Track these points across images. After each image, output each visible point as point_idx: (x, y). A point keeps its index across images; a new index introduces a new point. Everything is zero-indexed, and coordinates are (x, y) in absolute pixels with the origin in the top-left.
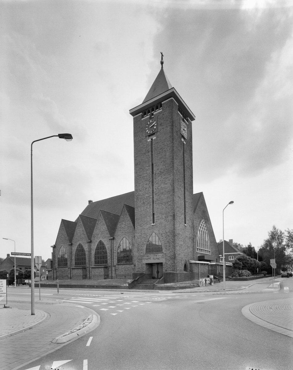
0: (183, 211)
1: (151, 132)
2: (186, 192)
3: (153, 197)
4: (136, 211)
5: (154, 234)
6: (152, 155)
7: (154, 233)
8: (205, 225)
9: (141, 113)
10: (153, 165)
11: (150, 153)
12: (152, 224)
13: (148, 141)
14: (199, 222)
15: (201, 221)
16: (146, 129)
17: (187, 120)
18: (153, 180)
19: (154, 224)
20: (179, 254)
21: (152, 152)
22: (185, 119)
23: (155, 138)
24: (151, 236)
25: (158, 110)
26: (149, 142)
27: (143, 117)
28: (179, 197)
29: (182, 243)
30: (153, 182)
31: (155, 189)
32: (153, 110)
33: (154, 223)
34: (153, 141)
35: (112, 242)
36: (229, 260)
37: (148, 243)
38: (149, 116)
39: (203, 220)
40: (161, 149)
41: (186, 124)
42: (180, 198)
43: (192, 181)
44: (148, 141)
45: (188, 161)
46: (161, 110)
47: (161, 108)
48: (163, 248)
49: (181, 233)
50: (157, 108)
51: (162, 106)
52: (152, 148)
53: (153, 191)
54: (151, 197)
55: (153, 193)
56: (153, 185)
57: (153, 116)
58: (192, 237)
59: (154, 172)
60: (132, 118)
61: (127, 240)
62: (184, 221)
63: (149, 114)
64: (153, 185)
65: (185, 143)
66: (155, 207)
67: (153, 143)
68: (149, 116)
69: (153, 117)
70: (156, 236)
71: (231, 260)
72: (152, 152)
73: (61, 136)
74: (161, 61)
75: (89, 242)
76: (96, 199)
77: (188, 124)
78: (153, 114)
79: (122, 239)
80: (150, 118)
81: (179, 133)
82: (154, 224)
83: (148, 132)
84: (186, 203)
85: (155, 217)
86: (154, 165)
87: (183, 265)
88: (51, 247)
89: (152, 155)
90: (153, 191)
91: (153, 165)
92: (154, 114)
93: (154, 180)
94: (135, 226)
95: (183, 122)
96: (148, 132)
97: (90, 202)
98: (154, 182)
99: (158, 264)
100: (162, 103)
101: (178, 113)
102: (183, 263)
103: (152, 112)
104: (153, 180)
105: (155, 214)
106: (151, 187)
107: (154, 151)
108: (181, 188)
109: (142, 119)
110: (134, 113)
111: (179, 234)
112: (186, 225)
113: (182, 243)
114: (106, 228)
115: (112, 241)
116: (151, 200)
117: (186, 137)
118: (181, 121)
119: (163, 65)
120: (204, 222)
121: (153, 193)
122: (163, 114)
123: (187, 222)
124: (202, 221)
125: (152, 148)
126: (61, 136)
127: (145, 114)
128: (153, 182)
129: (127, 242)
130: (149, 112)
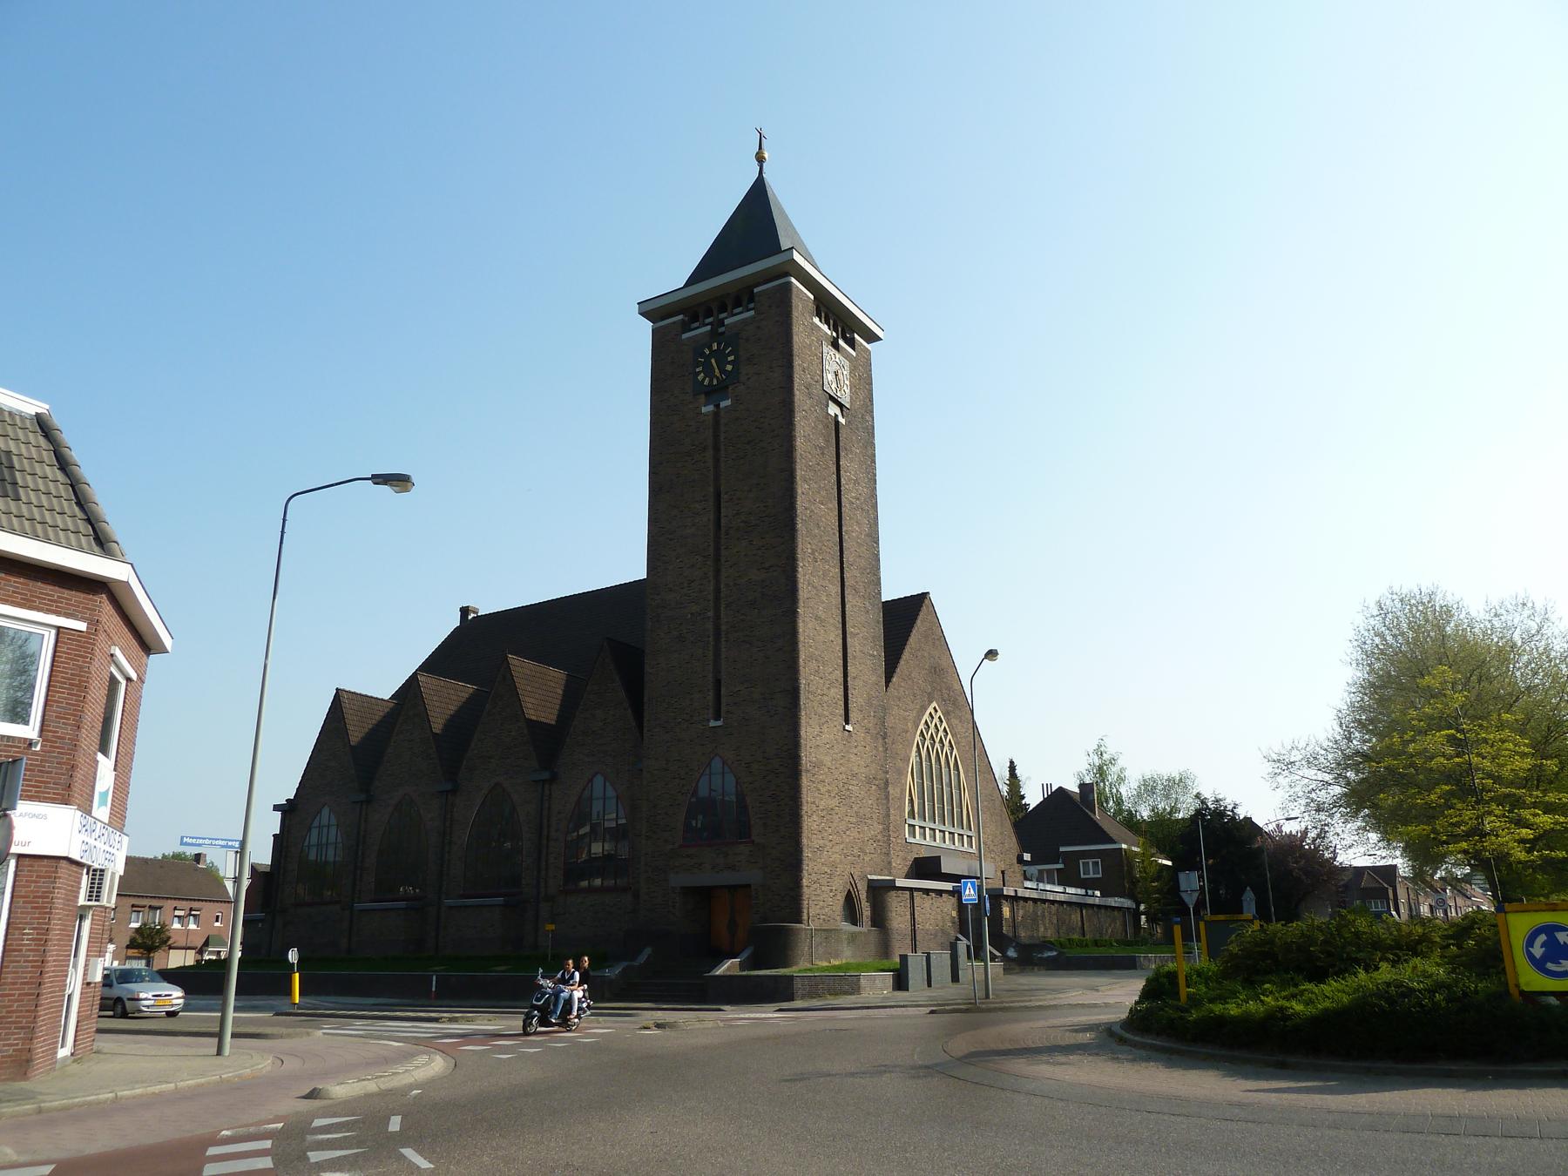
0: (839, 674)
1: (715, 382)
2: (848, 598)
3: (717, 617)
4: (647, 668)
5: (717, 764)
6: (717, 461)
7: (717, 758)
8: (944, 724)
9: (681, 317)
10: (718, 496)
11: (710, 453)
12: (713, 723)
13: (704, 410)
14: (915, 713)
15: (926, 709)
16: (697, 370)
17: (851, 343)
18: (717, 549)
19: (719, 723)
20: (821, 849)
21: (717, 449)
22: (841, 342)
23: (728, 402)
24: (707, 771)
25: (740, 309)
26: (705, 415)
27: (686, 327)
28: (817, 618)
29: (834, 803)
30: (717, 559)
31: (727, 585)
32: (723, 309)
33: (717, 718)
34: (722, 413)
35: (547, 792)
36: (1082, 876)
37: (693, 800)
38: (709, 328)
39: (934, 704)
40: (749, 443)
41: (847, 356)
42: (822, 621)
43: (878, 555)
44: (704, 410)
45: (856, 482)
46: (752, 313)
47: (752, 305)
48: (752, 822)
49: (827, 760)
50: (738, 303)
51: (756, 299)
52: (716, 436)
53: (717, 591)
54: (710, 614)
55: (717, 599)
56: (717, 572)
57: (722, 330)
58: (881, 775)
59: (723, 521)
60: (647, 326)
61: (607, 784)
62: (842, 712)
63: (710, 320)
64: (717, 572)
65: (842, 420)
66: (723, 656)
67: (723, 421)
68: (709, 328)
69: (724, 333)
70: (726, 768)
71: (1091, 876)
72: (717, 449)
73: (379, 479)
74: (757, 153)
75: (447, 791)
76: (488, 604)
77: (854, 354)
78: (721, 323)
79: (591, 781)
80: (714, 335)
81: (816, 391)
82: (719, 723)
83: (704, 380)
84: (849, 640)
85: (722, 692)
86: (724, 497)
87: (841, 898)
88: (276, 808)
89: (717, 461)
90: (717, 591)
91: (718, 496)
92: (726, 322)
93: (723, 552)
94: (645, 731)
95: (833, 351)
96: (704, 380)
97: (465, 611)
98: (723, 559)
99: (733, 888)
100: (756, 290)
101: (813, 323)
102: (839, 886)
103: (722, 316)
104: (717, 549)
105: (723, 682)
106: (711, 578)
107: (722, 447)
108: (826, 583)
109: (685, 336)
110: (653, 311)
111: (818, 765)
112: (848, 727)
113: (834, 803)
114: (526, 731)
115: (547, 786)
116: (710, 626)
117: (848, 399)
118: (828, 351)
119: (764, 164)
120: (939, 713)
121: (717, 599)
122: (759, 327)
123: (853, 715)
124: (930, 709)
125: (716, 436)
126: (379, 479)
127: (695, 318)
128: (717, 559)
129: (610, 792)
130: (709, 313)
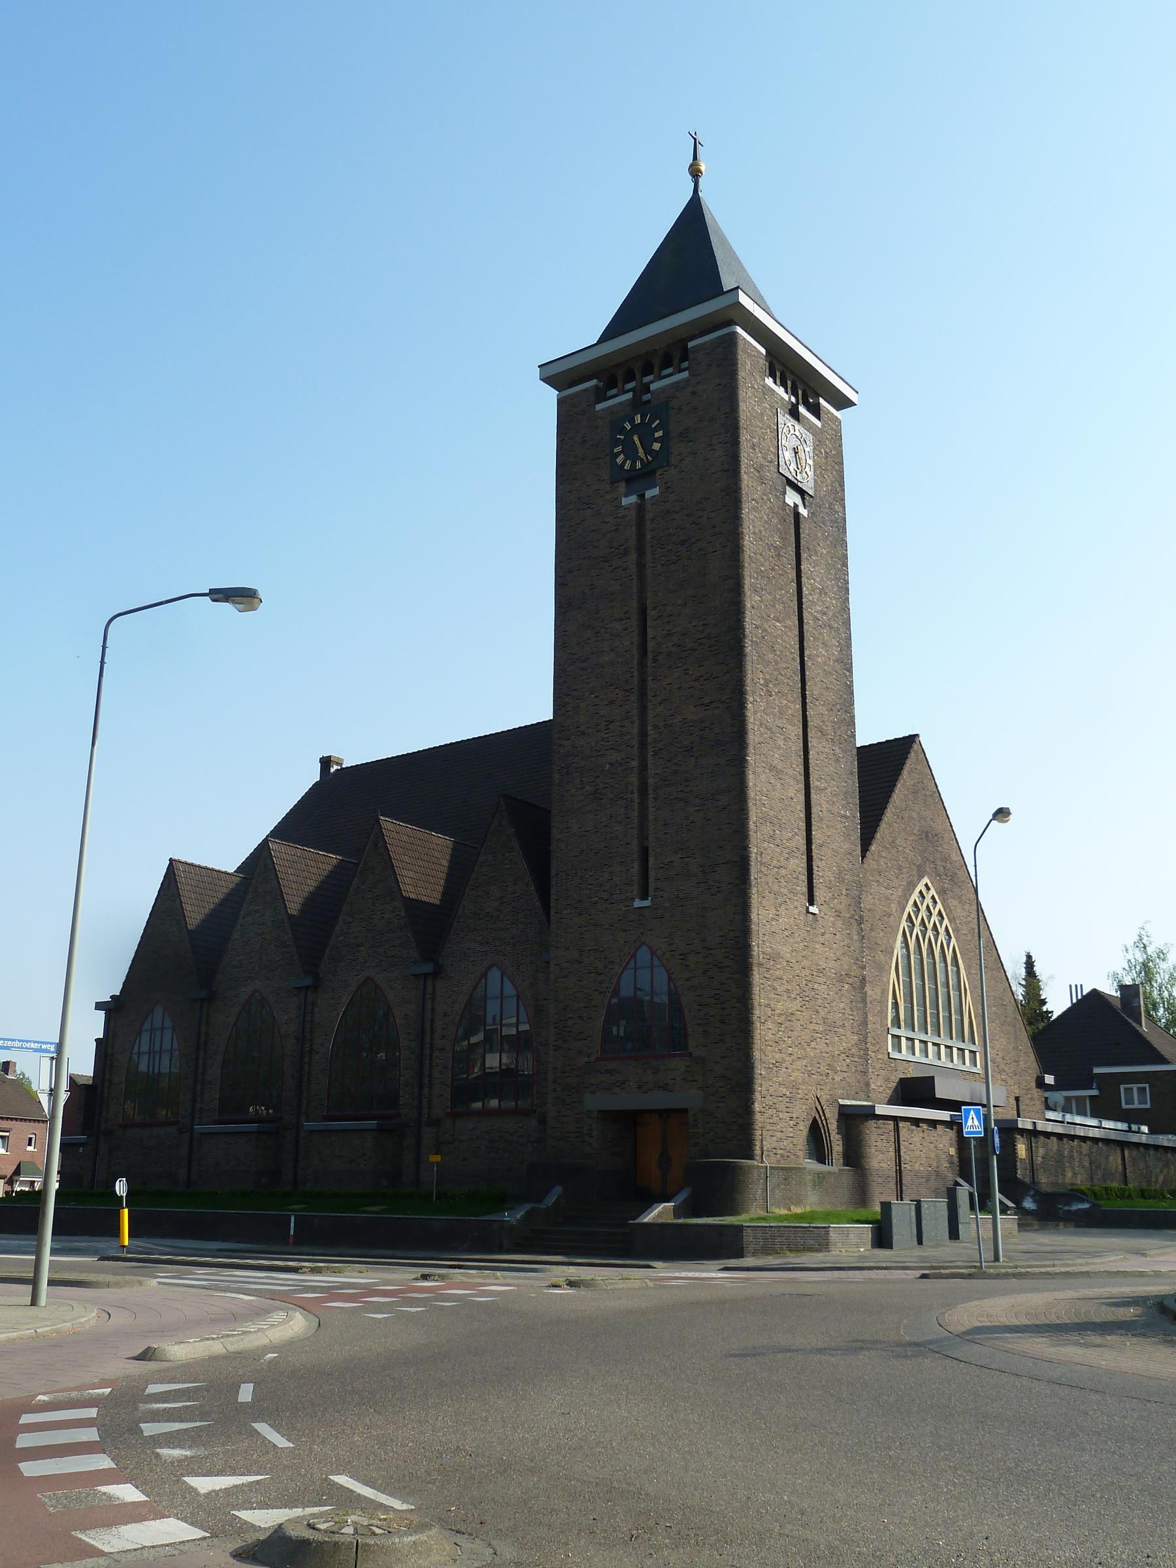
0: (801, 841)
1: (638, 465)
2: (812, 742)
3: (643, 768)
4: (555, 834)
5: (644, 955)
6: (641, 566)
7: (645, 948)
8: (939, 906)
9: (594, 382)
10: (643, 612)
11: (633, 557)
12: (638, 903)
13: (625, 501)
14: (900, 892)
15: (915, 886)
16: (616, 450)
17: (816, 410)
18: (643, 681)
19: (647, 903)
20: (777, 1064)
21: (641, 552)
24: (632, 964)
27: (600, 395)
28: (772, 768)
29: (794, 1006)
30: (643, 694)
31: (656, 727)
32: (648, 369)
33: (644, 896)
34: (648, 505)
35: (430, 989)
36: (1124, 1106)
37: (615, 1001)
38: (629, 395)
39: (926, 880)
40: (683, 543)
41: (810, 427)
42: (779, 772)
44: (625, 501)
45: (823, 592)
46: (686, 374)
47: (685, 365)
48: (690, 1029)
49: (785, 951)
50: (667, 362)
51: (691, 356)
52: (641, 536)
53: (643, 734)
54: (635, 764)
55: (643, 745)
56: (643, 709)
58: (855, 971)
60: (551, 395)
61: (505, 979)
62: (805, 890)
64: (643, 709)
65: (803, 511)
66: (651, 818)
67: (649, 516)
68: (629, 395)
70: (656, 962)
71: (1136, 1105)
72: (641, 552)
73: (220, 595)
74: (691, 166)
75: (307, 988)
78: (646, 388)
79: (484, 975)
80: (637, 404)
81: (770, 474)
82: (647, 903)
83: (624, 463)
84: (813, 796)
86: (651, 614)
87: (804, 1129)
88: (99, 1006)
89: (641, 566)
90: (643, 734)
91: (643, 612)
92: (653, 387)
93: (650, 684)
94: (552, 913)
95: (791, 422)
96: (624, 463)
97: (326, 762)
99: (665, 1114)
100: (691, 344)
101: (765, 386)
102: (802, 1112)
103: (647, 379)
104: (643, 681)
105: (651, 851)
106: (635, 718)
107: (649, 550)
109: (599, 407)
111: (775, 957)
112: (813, 909)
113: (794, 1006)
114: (403, 914)
115: (430, 982)
116: (634, 779)
117: (811, 484)
118: (785, 420)
120: (933, 892)
121: (643, 745)
122: (694, 393)
123: (820, 893)
124: (921, 887)
125: (641, 536)
126: (220, 595)
127: (611, 383)
128: (643, 694)
129: (509, 989)
130: (630, 377)
